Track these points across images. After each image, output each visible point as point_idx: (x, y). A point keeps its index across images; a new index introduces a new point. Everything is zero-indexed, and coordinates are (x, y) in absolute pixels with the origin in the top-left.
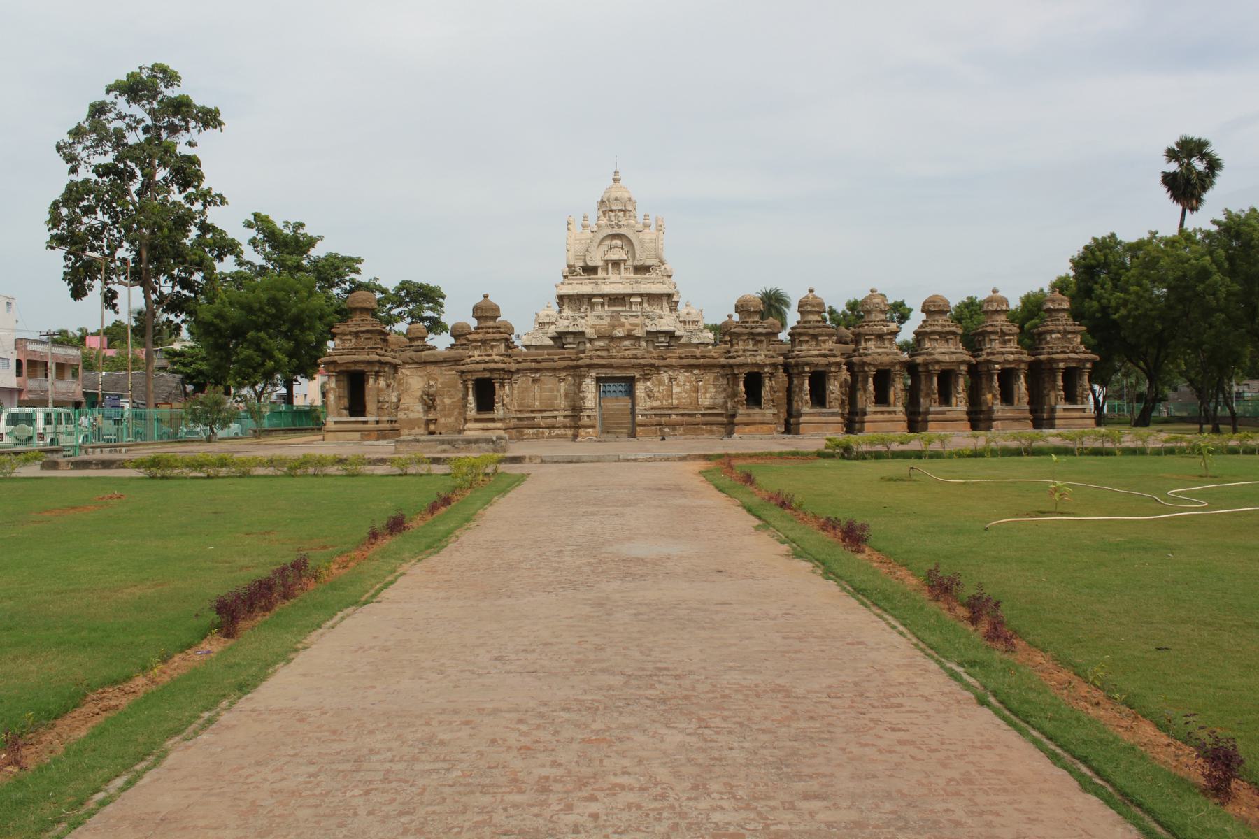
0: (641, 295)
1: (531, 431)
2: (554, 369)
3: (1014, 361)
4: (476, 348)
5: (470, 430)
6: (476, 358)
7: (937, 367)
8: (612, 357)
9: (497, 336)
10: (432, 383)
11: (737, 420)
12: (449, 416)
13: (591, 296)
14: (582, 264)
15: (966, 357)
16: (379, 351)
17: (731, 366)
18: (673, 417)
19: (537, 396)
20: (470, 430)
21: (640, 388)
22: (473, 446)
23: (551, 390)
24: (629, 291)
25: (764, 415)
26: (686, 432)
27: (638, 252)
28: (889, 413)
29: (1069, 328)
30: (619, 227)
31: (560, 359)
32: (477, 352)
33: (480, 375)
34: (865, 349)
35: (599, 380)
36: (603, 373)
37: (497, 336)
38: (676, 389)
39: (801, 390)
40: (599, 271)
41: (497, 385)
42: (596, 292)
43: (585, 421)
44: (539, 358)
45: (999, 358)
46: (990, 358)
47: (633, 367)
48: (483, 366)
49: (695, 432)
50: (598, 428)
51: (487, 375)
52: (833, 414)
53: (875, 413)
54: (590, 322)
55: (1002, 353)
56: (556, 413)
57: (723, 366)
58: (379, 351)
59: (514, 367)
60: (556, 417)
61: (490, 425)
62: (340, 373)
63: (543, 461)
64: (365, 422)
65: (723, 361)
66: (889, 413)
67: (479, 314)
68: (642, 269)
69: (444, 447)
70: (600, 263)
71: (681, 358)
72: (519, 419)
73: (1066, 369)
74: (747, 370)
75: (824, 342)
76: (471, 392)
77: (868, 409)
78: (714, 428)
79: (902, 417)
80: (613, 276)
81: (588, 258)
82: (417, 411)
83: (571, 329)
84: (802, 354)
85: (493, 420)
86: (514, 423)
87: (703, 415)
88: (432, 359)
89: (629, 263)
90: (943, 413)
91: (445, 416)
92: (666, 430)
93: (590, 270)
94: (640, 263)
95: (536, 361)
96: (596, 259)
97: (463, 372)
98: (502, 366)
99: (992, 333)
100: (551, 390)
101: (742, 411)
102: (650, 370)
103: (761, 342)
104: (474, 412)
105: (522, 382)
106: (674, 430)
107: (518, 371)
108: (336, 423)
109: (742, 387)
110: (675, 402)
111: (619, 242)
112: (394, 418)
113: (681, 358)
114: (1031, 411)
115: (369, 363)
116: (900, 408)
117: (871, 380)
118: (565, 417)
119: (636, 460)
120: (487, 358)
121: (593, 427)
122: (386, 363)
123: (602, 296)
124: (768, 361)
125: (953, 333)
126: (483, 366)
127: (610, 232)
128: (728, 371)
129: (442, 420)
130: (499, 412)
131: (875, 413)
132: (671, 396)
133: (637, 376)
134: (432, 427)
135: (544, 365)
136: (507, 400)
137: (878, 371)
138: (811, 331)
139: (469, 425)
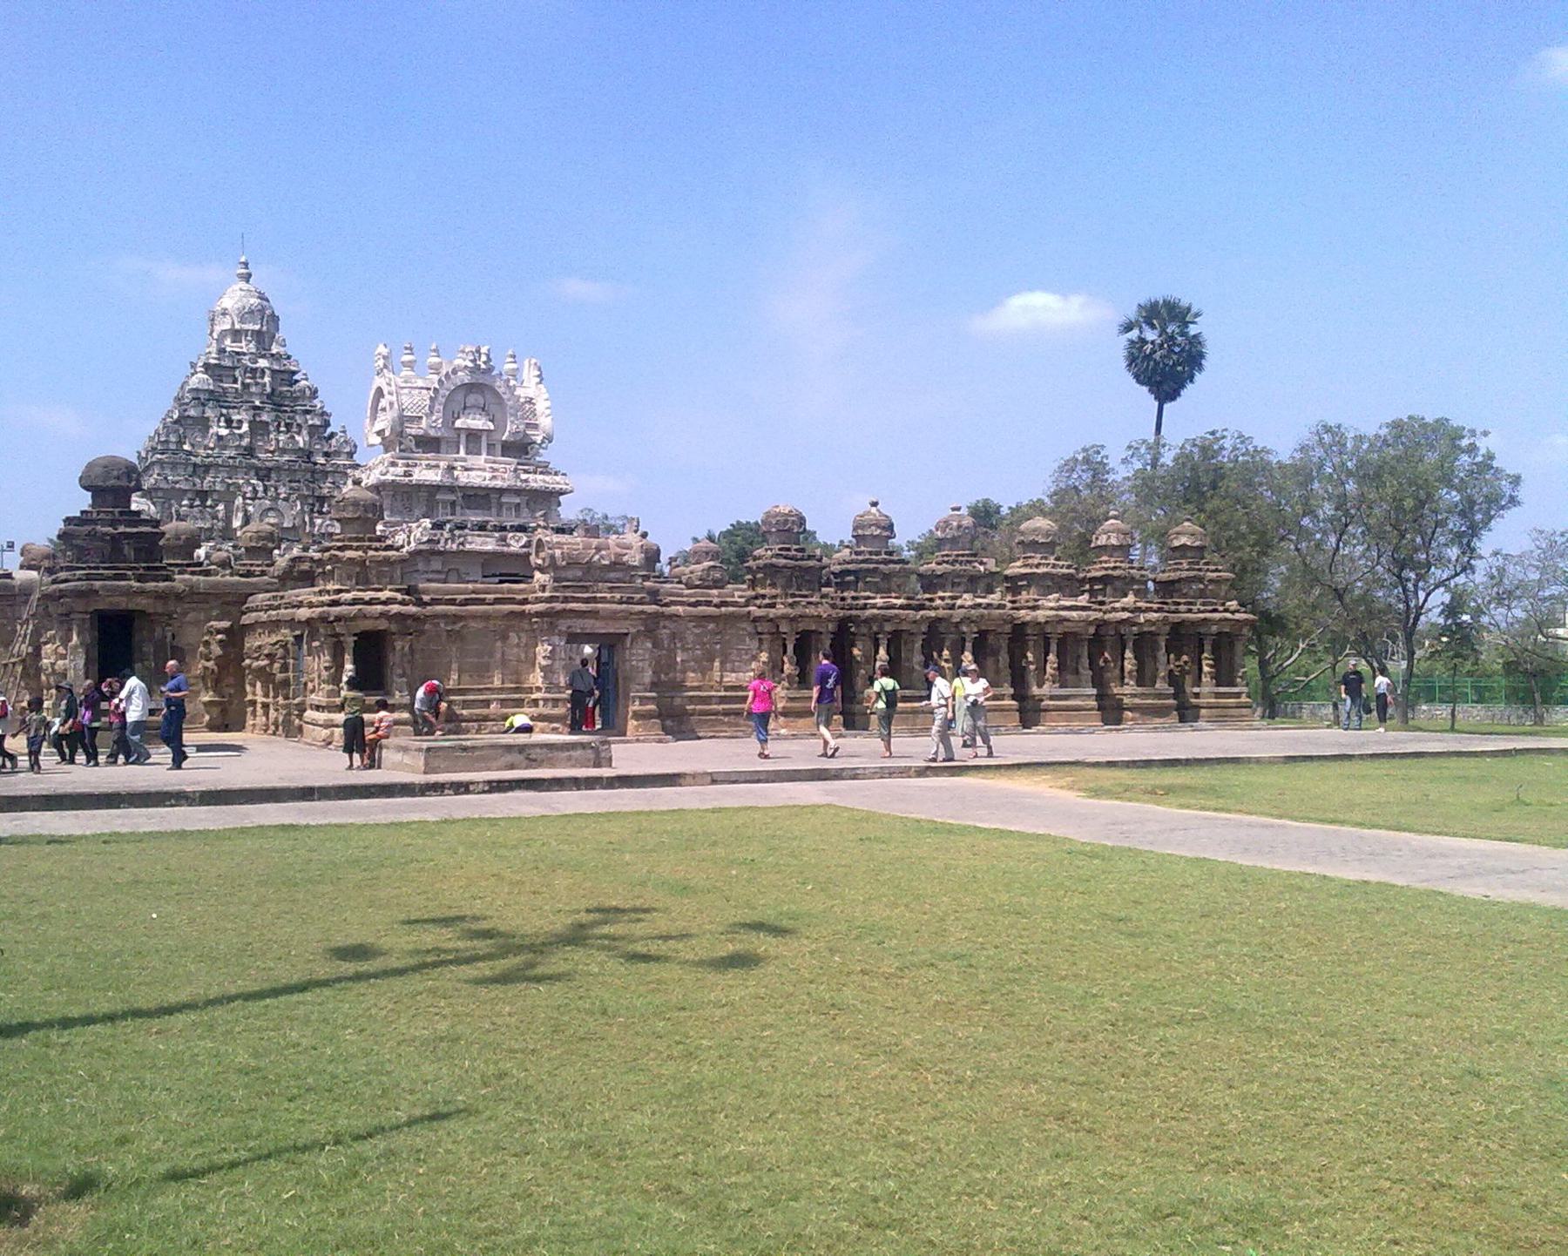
2: (486, 617)
8: (595, 600)
13: (434, 489)
31: (497, 601)
40: (443, 447)
42: (448, 481)
51: (383, 625)
74: (801, 627)
83: (440, 547)
87: (723, 700)
93: (429, 444)
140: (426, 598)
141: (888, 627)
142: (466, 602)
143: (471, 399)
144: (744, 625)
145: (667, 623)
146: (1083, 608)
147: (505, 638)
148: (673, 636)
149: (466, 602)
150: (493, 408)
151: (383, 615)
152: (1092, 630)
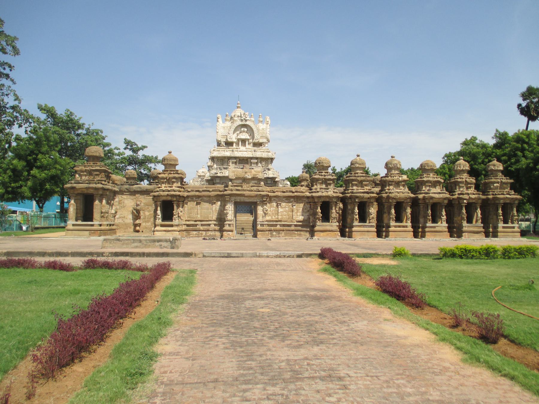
1: (195, 232)
4: (163, 183)
5: (157, 231)
6: (163, 188)
7: (431, 201)
9: (176, 175)
10: (138, 203)
11: (317, 228)
12: (148, 222)
13: (229, 158)
14: (224, 140)
15: (447, 195)
16: (103, 182)
17: (313, 197)
18: (278, 226)
20: (157, 231)
21: (260, 210)
22: (157, 244)
23: (208, 209)
24: (251, 156)
25: (332, 226)
26: (286, 235)
27: (256, 135)
28: (404, 227)
29: (503, 181)
30: (246, 121)
32: (163, 185)
33: (164, 198)
34: (389, 190)
36: (238, 199)
37: (176, 175)
39: (353, 212)
40: (234, 144)
43: (227, 227)
44: (201, 190)
45: (466, 197)
46: (461, 196)
47: (256, 196)
48: (167, 193)
49: (291, 235)
50: (235, 232)
51: (169, 198)
52: (372, 226)
53: (395, 226)
54: (231, 171)
55: (468, 194)
56: (210, 223)
57: (308, 197)
58: (103, 182)
59: (186, 194)
60: (209, 225)
61: (170, 229)
62: (78, 194)
63: (204, 256)
64: (92, 225)
65: (308, 194)
66: (404, 227)
67: (166, 162)
68: (258, 145)
69: (136, 244)
70: (235, 140)
71: (284, 192)
72: (188, 225)
73: (504, 204)
74: (322, 200)
75: (366, 185)
76: (159, 208)
77: (391, 224)
78: (302, 233)
79: (410, 229)
80: (242, 148)
81: (228, 137)
82: (129, 219)
83: (219, 175)
84: (355, 191)
85: (172, 226)
86: (184, 227)
88: (139, 190)
89: (251, 141)
90: (434, 227)
91: (145, 222)
92: (274, 233)
93: (229, 144)
94: (257, 141)
95: (198, 191)
96: (233, 138)
97: (154, 196)
98: (178, 193)
99: (460, 182)
100: (208, 209)
101: (319, 223)
102: (266, 199)
103: (330, 184)
104: (160, 220)
105: (191, 205)
106: (279, 234)
107: (188, 197)
108: (73, 225)
109: (319, 210)
110: (280, 217)
111: (246, 129)
112: (112, 223)
113: (284, 192)
114: (484, 228)
115: (96, 189)
116: (409, 224)
118: (215, 225)
119: (268, 257)
120: (169, 189)
121: (232, 231)
122: (108, 190)
123: (235, 158)
124: (335, 195)
125: (439, 182)
126: (167, 193)
127: (241, 123)
128: (311, 200)
129: (143, 224)
130: (176, 222)
131: (395, 226)
134: (138, 228)
135: (204, 193)
136: (181, 214)
138: (359, 178)
139: (158, 228)
140: (189, 190)
143: (242, 129)
144: (305, 199)
145: (275, 198)
149: (204, 191)
151: (168, 195)
152: (446, 202)
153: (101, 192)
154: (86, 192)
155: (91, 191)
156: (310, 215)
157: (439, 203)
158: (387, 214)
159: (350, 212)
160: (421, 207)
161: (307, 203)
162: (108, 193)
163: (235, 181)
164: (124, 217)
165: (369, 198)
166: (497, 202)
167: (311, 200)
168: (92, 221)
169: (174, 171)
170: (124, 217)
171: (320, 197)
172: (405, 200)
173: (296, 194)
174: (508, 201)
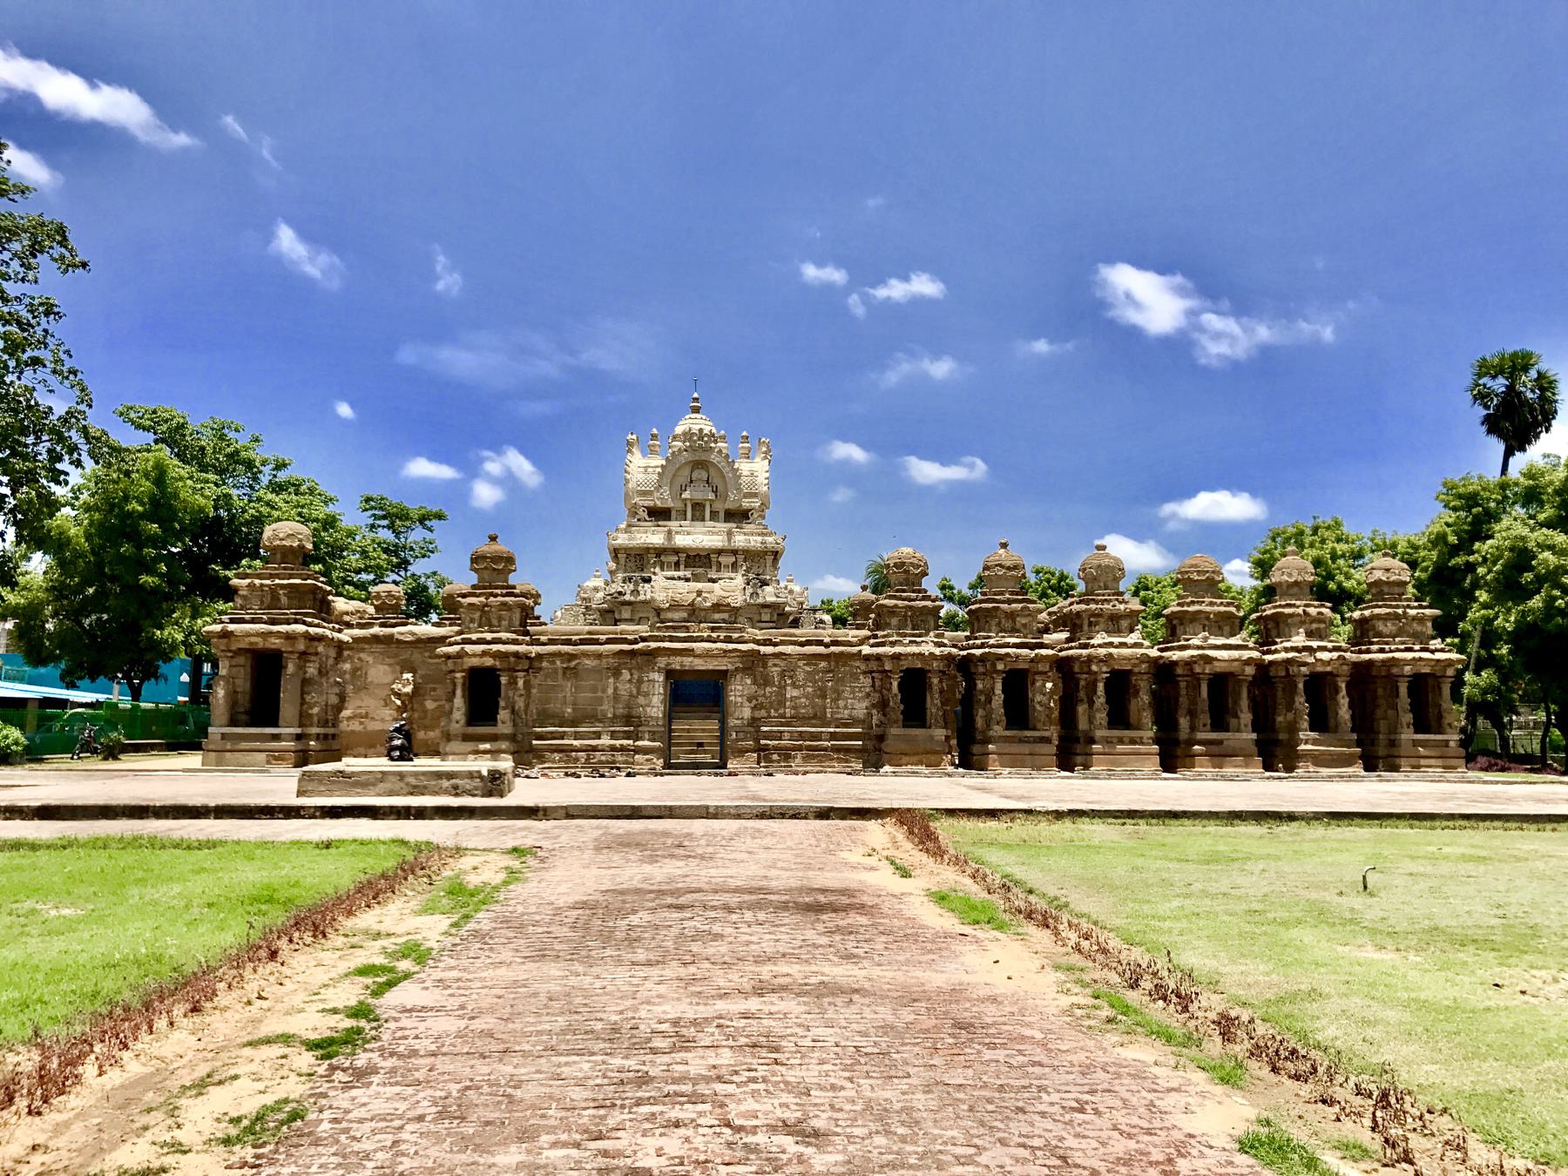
0: (735, 552)
2: (599, 656)
3: (1329, 663)
19: (569, 699)
22: (446, 784)
25: (932, 737)
31: (609, 641)
33: (475, 662)
35: (669, 674)
36: (677, 663)
38: (791, 692)
41: (504, 680)
51: (489, 662)
57: (867, 658)
62: (240, 651)
64: (276, 737)
65: (866, 650)
74: (905, 665)
76: (459, 692)
90: (1220, 742)
91: (426, 728)
112: (331, 731)
113: (802, 644)
115: (289, 637)
117: (1101, 686)
128: (873, 665)
132: (782, 703)
133: (730, 667)
137: (1113, 672)
141: (1000, 667)
142: (583, 642)
144: (857, 664)
145: (777, 661)
146: (1238, 647)
147: (617, 673)
148: (782, 675)
149: (583, 642)
150: (716, 481)
151: (484, 654)
152: (1250, 670)
153: (301, 646)
154: (261, 645)
155: (275, 643)
156: (873, 706)
157: (1231, 674)
158: (1086, 706)
159: (983, 698)
160: (1183, 685)
161: (865, 673)
162: (320, 649)
163: (670, 615)
164: (366, 716)
165: (1032, 660)
166: (1395, 671)
167: (873, 665)
168: (276, 725)
169: (502, 587)
170: (366, 716)
171: (896, 657)
172: (1135, 665)
173: (833, 649)
174: (1427, 670)
